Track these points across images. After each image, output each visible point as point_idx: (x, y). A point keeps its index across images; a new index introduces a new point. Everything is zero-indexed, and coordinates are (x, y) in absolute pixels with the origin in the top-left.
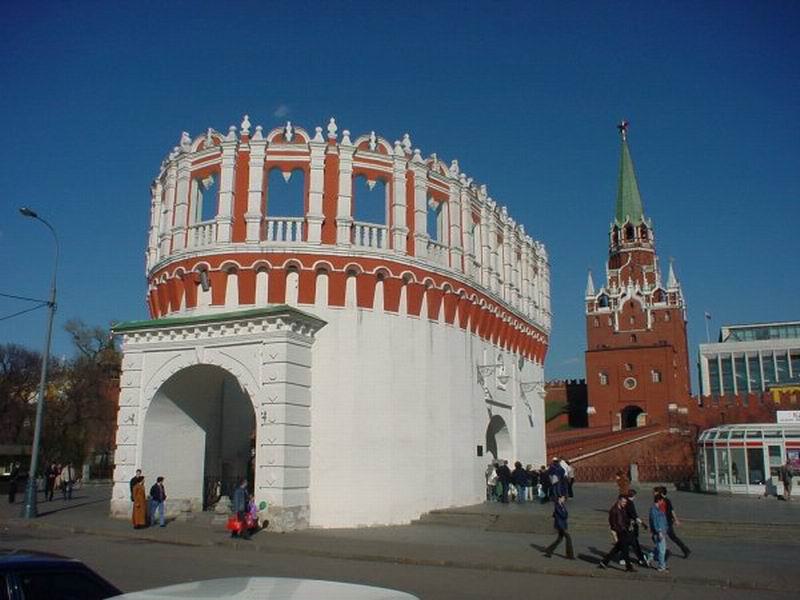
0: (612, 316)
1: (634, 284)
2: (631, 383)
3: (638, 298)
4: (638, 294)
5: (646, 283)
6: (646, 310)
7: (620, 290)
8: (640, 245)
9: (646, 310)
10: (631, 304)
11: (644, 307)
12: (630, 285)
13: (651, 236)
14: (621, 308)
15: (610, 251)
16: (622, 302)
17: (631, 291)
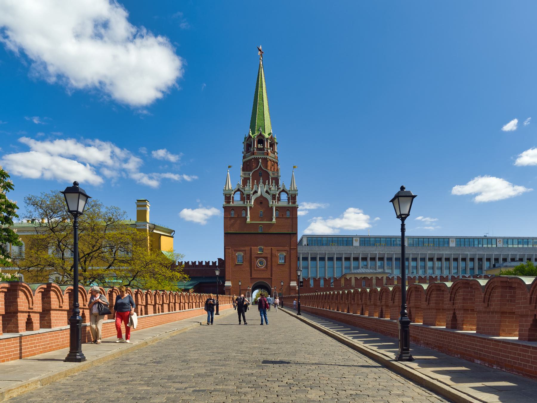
0: (245, 209)
2: (261, 263)
3: (266, 195)
4: (267, 192)
5: (274, 184)
6: (272, 207)
7: (252, 189)
9: (272, 207)
10: (261, 201)
12: (261, 184)
15: (244, 157)
17: (261, 190)
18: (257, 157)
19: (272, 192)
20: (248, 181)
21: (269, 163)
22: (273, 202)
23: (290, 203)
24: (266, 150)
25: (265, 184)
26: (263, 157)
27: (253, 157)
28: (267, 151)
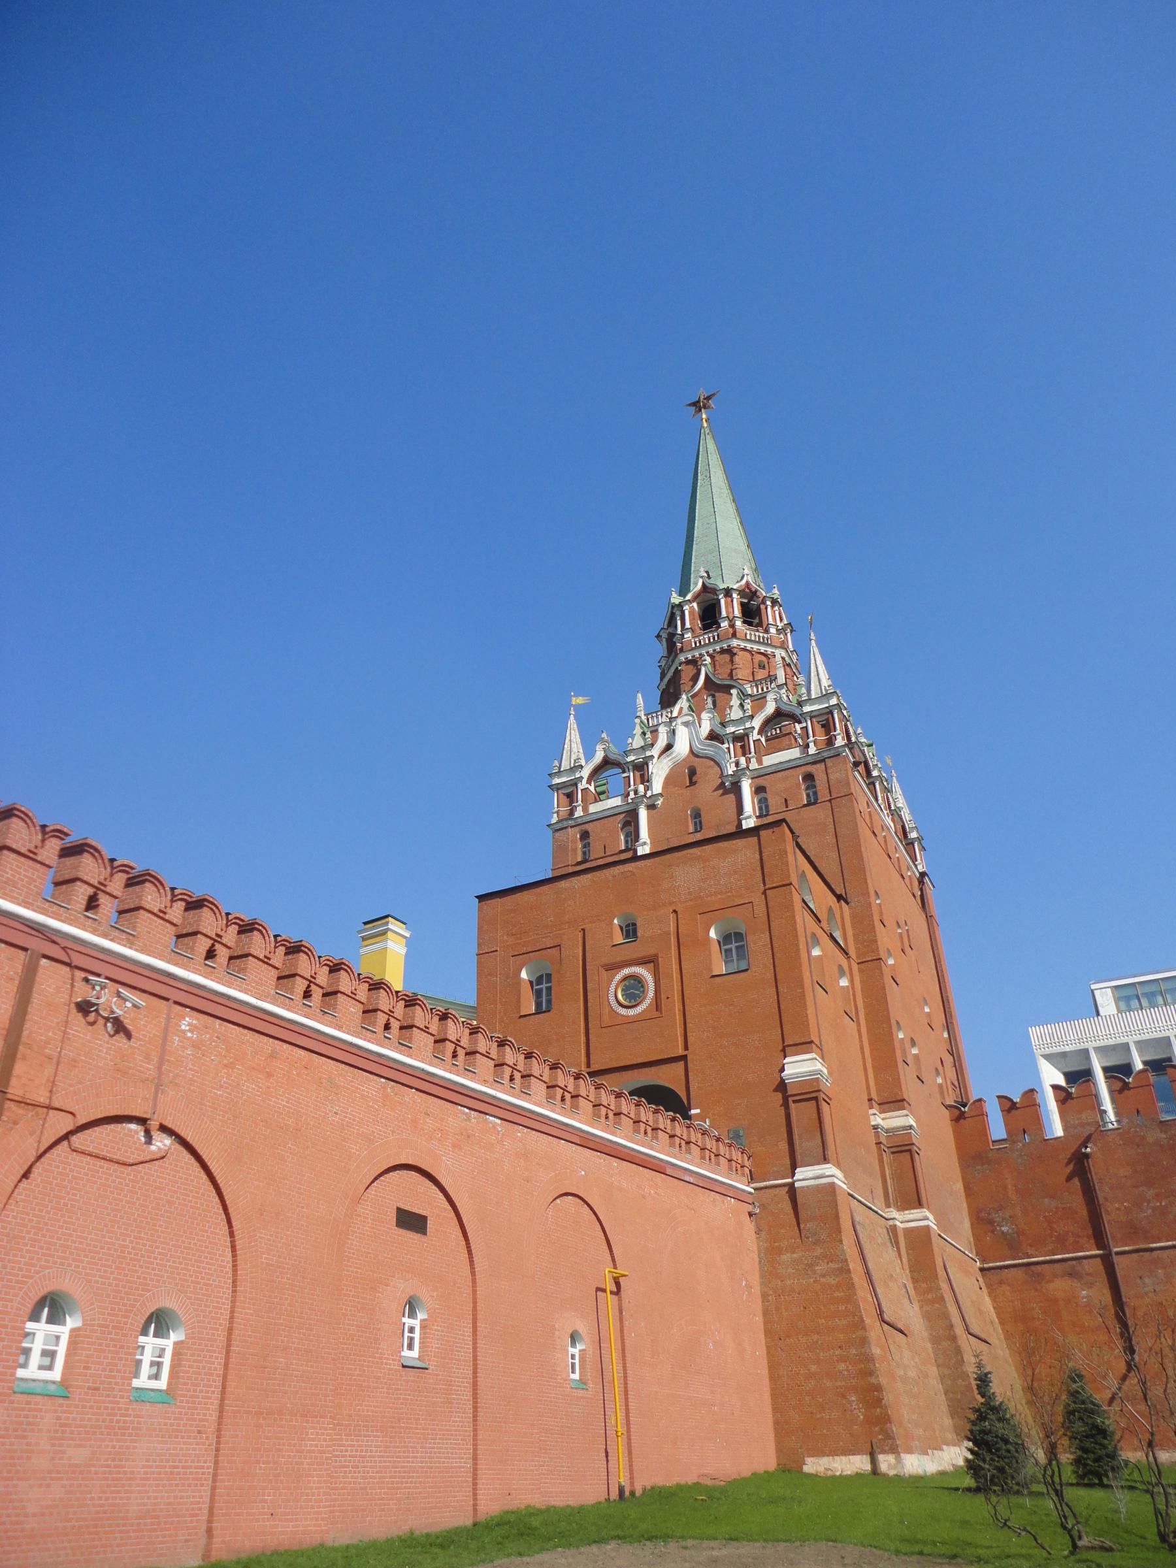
0: (630, 819)
1: (696, 710)
2: (634, 987)
8: (734, 635)
13: (771, 615)
14: (657, 787)
16: (659, 771)
19: (731, 729)
21: (741, 659)
22: (737, 764)
23: (812, 750)
24: (724, 624)
26: (718, 648)
28: (732, 626)
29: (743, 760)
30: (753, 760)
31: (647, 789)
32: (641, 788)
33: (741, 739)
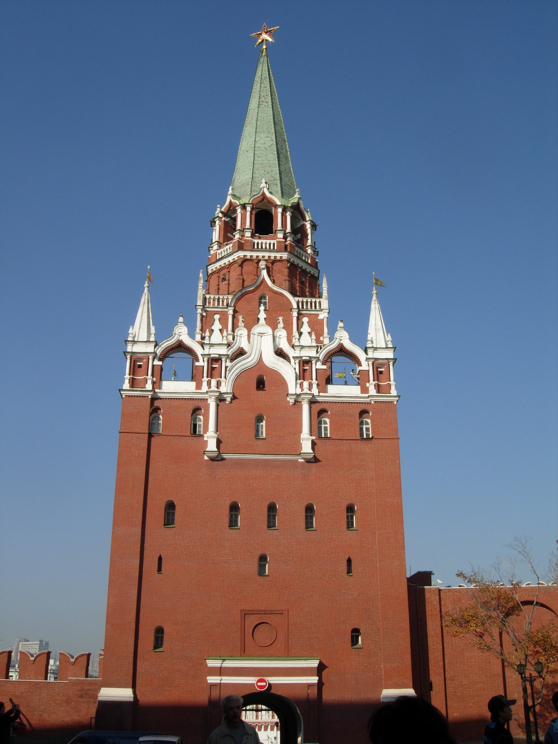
5: (306, 329)
11: (299, 391)
12: (262, 327)
17: (261, 343)
18: (255, 254)
20: (217, 317)
25: (274, 327)
26: (273, 255)
27: (241, 254)
29: (306, 384)
30: (315, 386)
31: (219, 384)
32: (214, 382)
33: (305, 363)
